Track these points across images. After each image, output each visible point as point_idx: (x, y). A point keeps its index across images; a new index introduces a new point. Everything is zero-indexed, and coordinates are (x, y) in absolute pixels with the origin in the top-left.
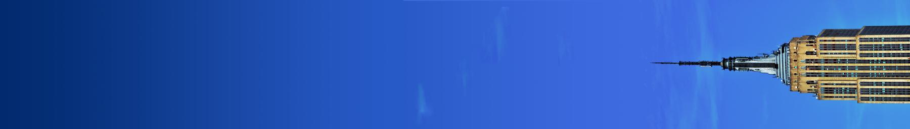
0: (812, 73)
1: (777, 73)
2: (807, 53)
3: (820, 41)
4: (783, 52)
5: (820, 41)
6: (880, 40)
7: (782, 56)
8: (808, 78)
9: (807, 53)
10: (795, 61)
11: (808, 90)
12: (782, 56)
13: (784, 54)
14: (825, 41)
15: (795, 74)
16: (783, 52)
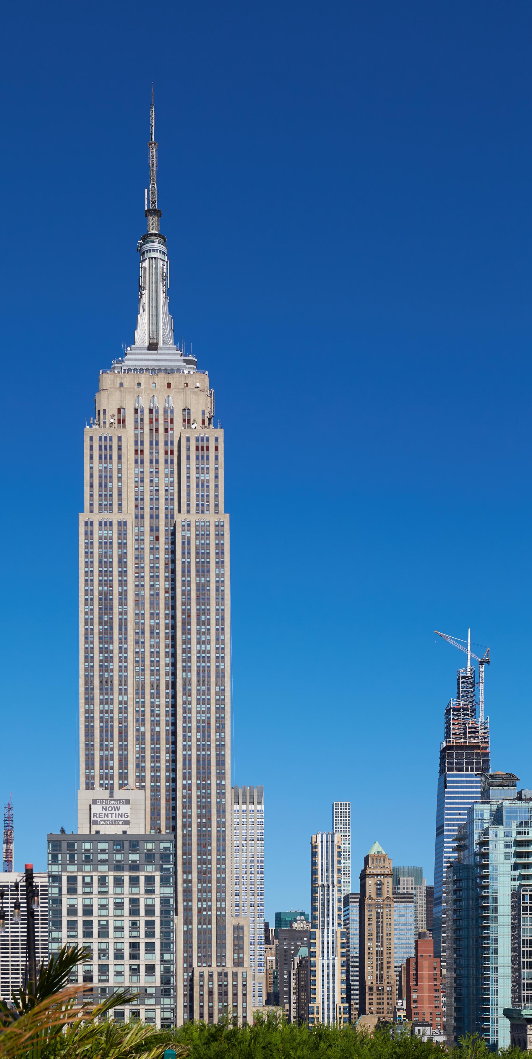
0: (142, 420)
1: (139, 348)
2: (186, 410)
3: (216, 439)
4: (185, 361)
5: (216, 439)
6: (220, 564)
7: (178, 360)
8: (133, 411)
9: (186, 410)
10: (169, 385)
11: (105, 411)
12: (178, 360)
13: (182, 363)
14: (216, 449)
15: (139, 384)
16: (185, 361)
